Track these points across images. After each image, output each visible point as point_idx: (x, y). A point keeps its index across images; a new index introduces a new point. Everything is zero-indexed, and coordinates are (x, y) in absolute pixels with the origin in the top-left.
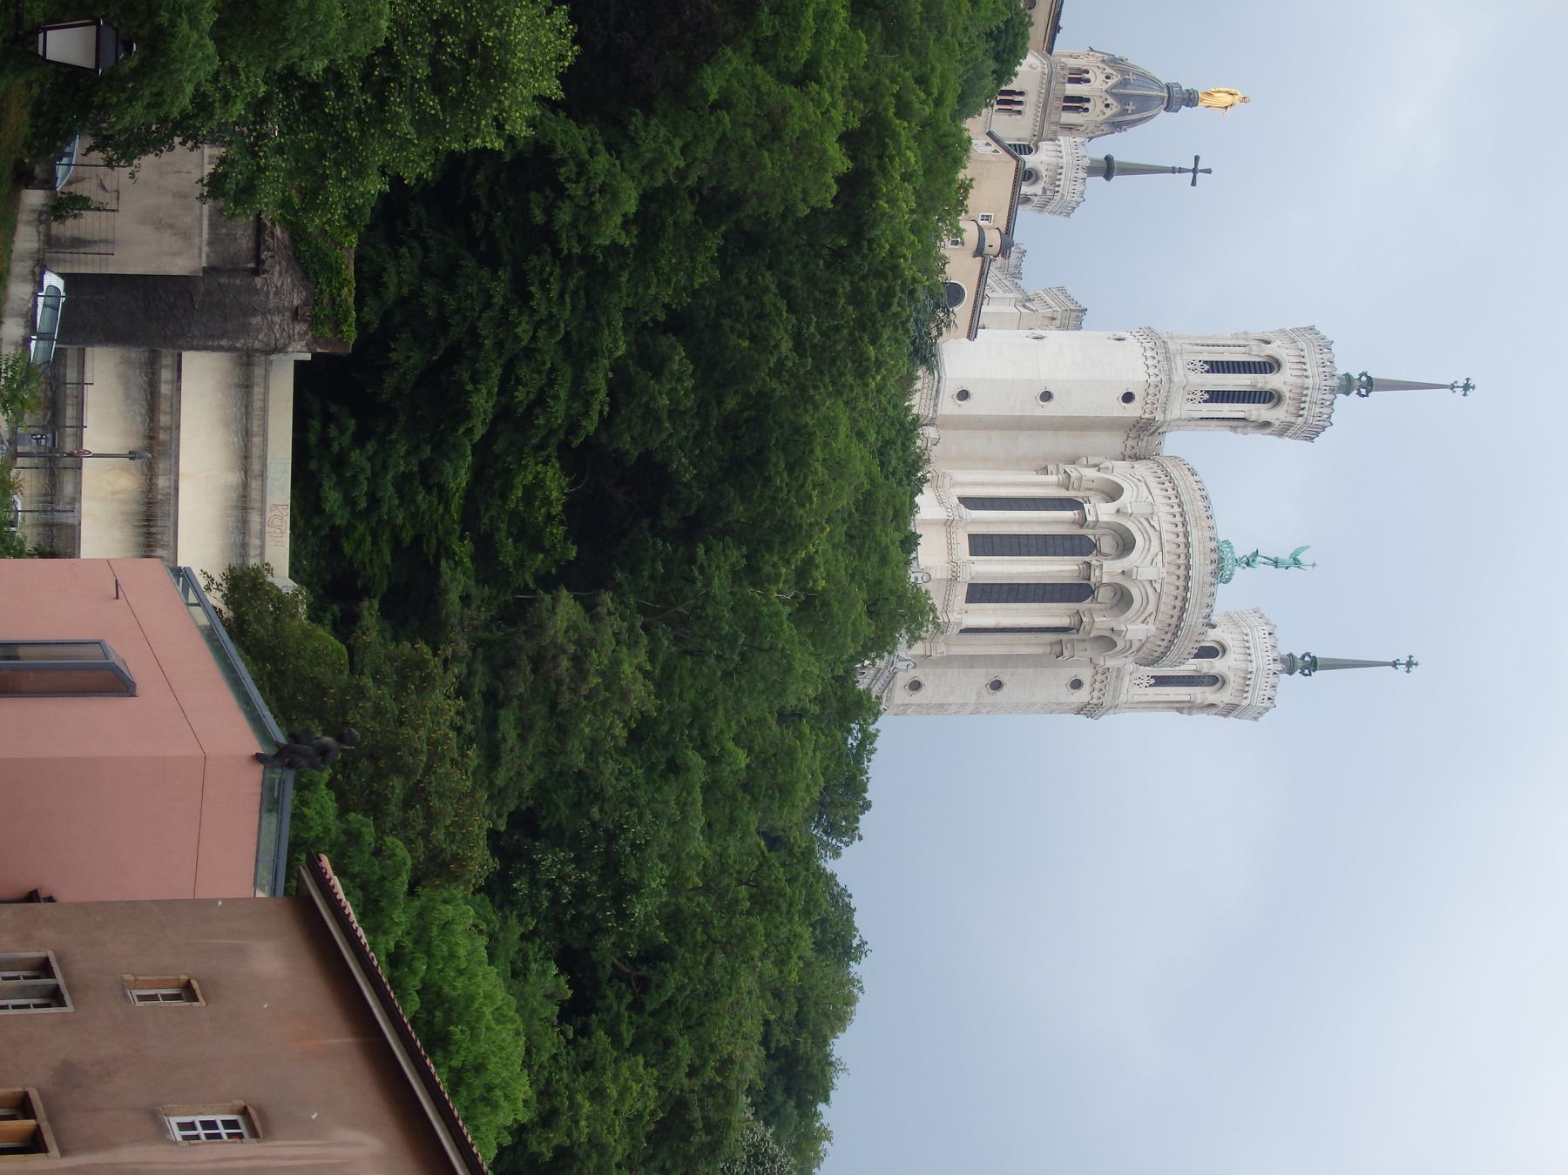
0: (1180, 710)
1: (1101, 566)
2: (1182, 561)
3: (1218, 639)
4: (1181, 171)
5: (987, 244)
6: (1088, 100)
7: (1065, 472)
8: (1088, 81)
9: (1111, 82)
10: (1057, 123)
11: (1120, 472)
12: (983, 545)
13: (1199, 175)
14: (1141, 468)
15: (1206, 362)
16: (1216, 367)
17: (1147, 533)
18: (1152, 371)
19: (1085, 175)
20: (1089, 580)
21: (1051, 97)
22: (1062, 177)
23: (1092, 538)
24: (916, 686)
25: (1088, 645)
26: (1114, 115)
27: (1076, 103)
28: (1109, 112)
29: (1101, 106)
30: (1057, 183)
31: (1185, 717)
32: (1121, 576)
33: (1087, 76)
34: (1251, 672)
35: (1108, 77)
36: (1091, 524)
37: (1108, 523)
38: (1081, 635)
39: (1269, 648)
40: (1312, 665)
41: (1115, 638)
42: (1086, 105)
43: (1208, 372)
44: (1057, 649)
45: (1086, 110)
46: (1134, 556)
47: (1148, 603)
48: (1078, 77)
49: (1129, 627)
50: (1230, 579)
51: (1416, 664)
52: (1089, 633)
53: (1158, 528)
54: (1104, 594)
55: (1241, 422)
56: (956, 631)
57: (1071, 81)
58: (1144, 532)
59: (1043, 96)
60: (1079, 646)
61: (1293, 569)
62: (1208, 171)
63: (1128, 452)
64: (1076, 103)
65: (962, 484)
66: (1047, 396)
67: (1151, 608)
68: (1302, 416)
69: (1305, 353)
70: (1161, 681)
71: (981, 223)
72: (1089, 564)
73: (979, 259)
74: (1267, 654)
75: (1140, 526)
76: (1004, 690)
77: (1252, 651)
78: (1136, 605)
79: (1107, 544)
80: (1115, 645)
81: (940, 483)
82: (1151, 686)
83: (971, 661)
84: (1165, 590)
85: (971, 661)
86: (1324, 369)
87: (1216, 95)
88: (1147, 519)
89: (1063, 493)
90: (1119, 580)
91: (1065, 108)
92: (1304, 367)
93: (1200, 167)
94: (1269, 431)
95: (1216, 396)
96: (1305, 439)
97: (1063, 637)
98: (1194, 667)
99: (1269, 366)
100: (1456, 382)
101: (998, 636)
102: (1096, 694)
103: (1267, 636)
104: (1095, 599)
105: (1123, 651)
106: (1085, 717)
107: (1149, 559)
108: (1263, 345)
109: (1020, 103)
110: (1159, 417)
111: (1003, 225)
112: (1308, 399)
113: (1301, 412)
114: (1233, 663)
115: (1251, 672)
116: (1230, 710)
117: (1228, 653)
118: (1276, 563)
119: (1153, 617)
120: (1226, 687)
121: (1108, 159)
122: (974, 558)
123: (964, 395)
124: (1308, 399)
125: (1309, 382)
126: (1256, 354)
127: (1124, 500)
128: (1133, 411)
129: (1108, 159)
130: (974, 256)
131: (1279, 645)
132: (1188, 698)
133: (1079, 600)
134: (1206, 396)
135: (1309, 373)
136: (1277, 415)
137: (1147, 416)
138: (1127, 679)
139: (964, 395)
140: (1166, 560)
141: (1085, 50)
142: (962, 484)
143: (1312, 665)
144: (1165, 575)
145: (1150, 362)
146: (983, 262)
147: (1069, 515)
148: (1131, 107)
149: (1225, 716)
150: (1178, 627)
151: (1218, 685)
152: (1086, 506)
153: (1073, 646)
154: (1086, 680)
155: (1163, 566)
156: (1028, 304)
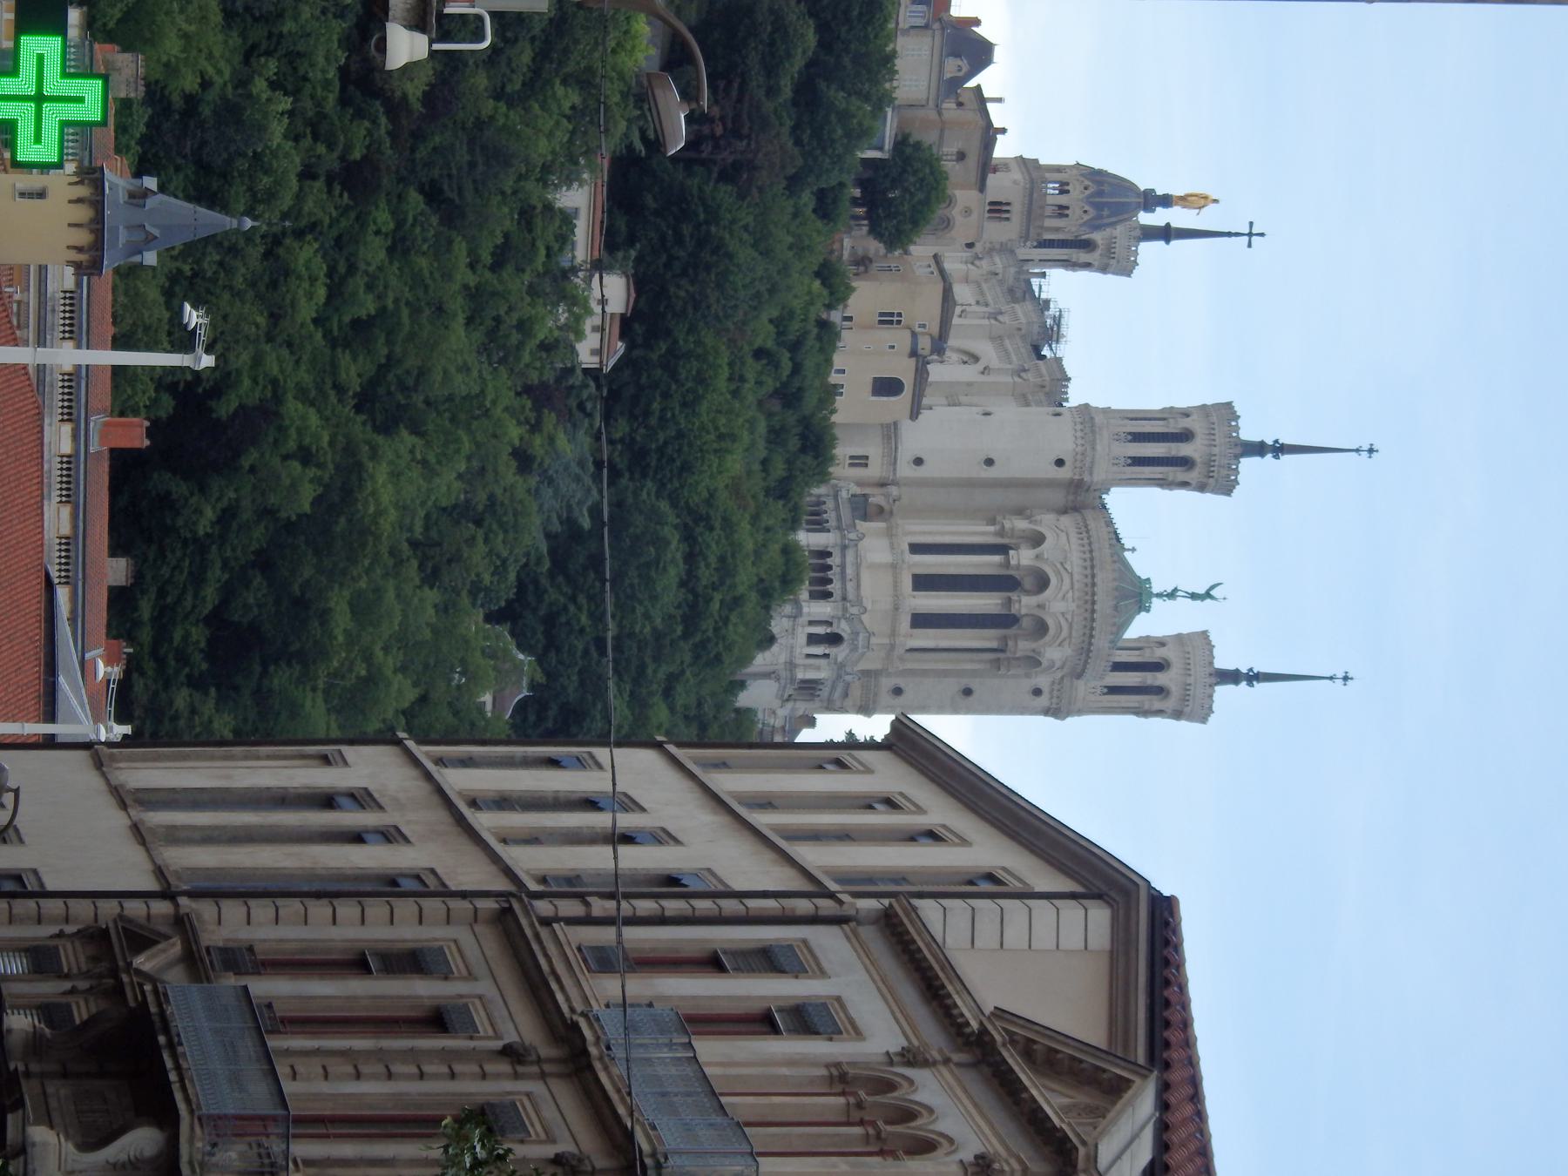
1: (1020, 601)
2: (1088, 598)
4: (1237, 234)
5: (920, 347)
6: (1067, 208)
9: (1087, 192)
11: (1046, 523)
12: (924, 582)
14: (1067, 521)
15: (1130, 433)
16: (1138, 437)
18: (1080, 441)
22: (1117, 245)
24: (898, 691)
26: (1091, 219)
28: (1086, 217)
29: (1079, 212)
31: (1142, 720)
35: (1086, 188)
38: (1008, 654)
42: (1066, 212)
43: (1130, 441)
45: (1067, 216)
46: (1048, 593)
51: (1352, 679)
54: (1026, 623)
55: (1163, 483)
56: (902, 651)
58: (1058, 573)
62: (1262, 235)
65: (914, 533)
67: (1065, 633)
69: (1215, 426)
71: (918, 330)
72: (1010, 599)
73: (914, 359)
78: (1052, 631)
79: (1028, 583)
80: (1039, 663)
81: (894, 532)
84: (1075, 620)
87: (1189, 198)
88: (1062, 564)
89: (999, 541)
92: (1213, 437)
98: (1139, 680)
99: (1185, 436)
101: (945, 655)
102: (1054, 700)
107: (1060, 595)
109: (1008, 211)
110: (1087, 478)
111: (935, 330)
112: (1216, 463)
113: (1211, 474)
116: (1178, 715)
118: (1194, 596)
119: (1067, 641)
122: (915, 593)
125: (1216, 450)
128: (1064, 473)
134: (1129, 461)
136: (1193, 476)
137: (1077, 477)
139: (919, 461)
145: (1079, 434)
146: (917, 362)
147: (997, 558)
148: (1106, 212)
150: (1089, 651)
154: (1046, 690)
155: (1073, 601)
156: (1023, 374)
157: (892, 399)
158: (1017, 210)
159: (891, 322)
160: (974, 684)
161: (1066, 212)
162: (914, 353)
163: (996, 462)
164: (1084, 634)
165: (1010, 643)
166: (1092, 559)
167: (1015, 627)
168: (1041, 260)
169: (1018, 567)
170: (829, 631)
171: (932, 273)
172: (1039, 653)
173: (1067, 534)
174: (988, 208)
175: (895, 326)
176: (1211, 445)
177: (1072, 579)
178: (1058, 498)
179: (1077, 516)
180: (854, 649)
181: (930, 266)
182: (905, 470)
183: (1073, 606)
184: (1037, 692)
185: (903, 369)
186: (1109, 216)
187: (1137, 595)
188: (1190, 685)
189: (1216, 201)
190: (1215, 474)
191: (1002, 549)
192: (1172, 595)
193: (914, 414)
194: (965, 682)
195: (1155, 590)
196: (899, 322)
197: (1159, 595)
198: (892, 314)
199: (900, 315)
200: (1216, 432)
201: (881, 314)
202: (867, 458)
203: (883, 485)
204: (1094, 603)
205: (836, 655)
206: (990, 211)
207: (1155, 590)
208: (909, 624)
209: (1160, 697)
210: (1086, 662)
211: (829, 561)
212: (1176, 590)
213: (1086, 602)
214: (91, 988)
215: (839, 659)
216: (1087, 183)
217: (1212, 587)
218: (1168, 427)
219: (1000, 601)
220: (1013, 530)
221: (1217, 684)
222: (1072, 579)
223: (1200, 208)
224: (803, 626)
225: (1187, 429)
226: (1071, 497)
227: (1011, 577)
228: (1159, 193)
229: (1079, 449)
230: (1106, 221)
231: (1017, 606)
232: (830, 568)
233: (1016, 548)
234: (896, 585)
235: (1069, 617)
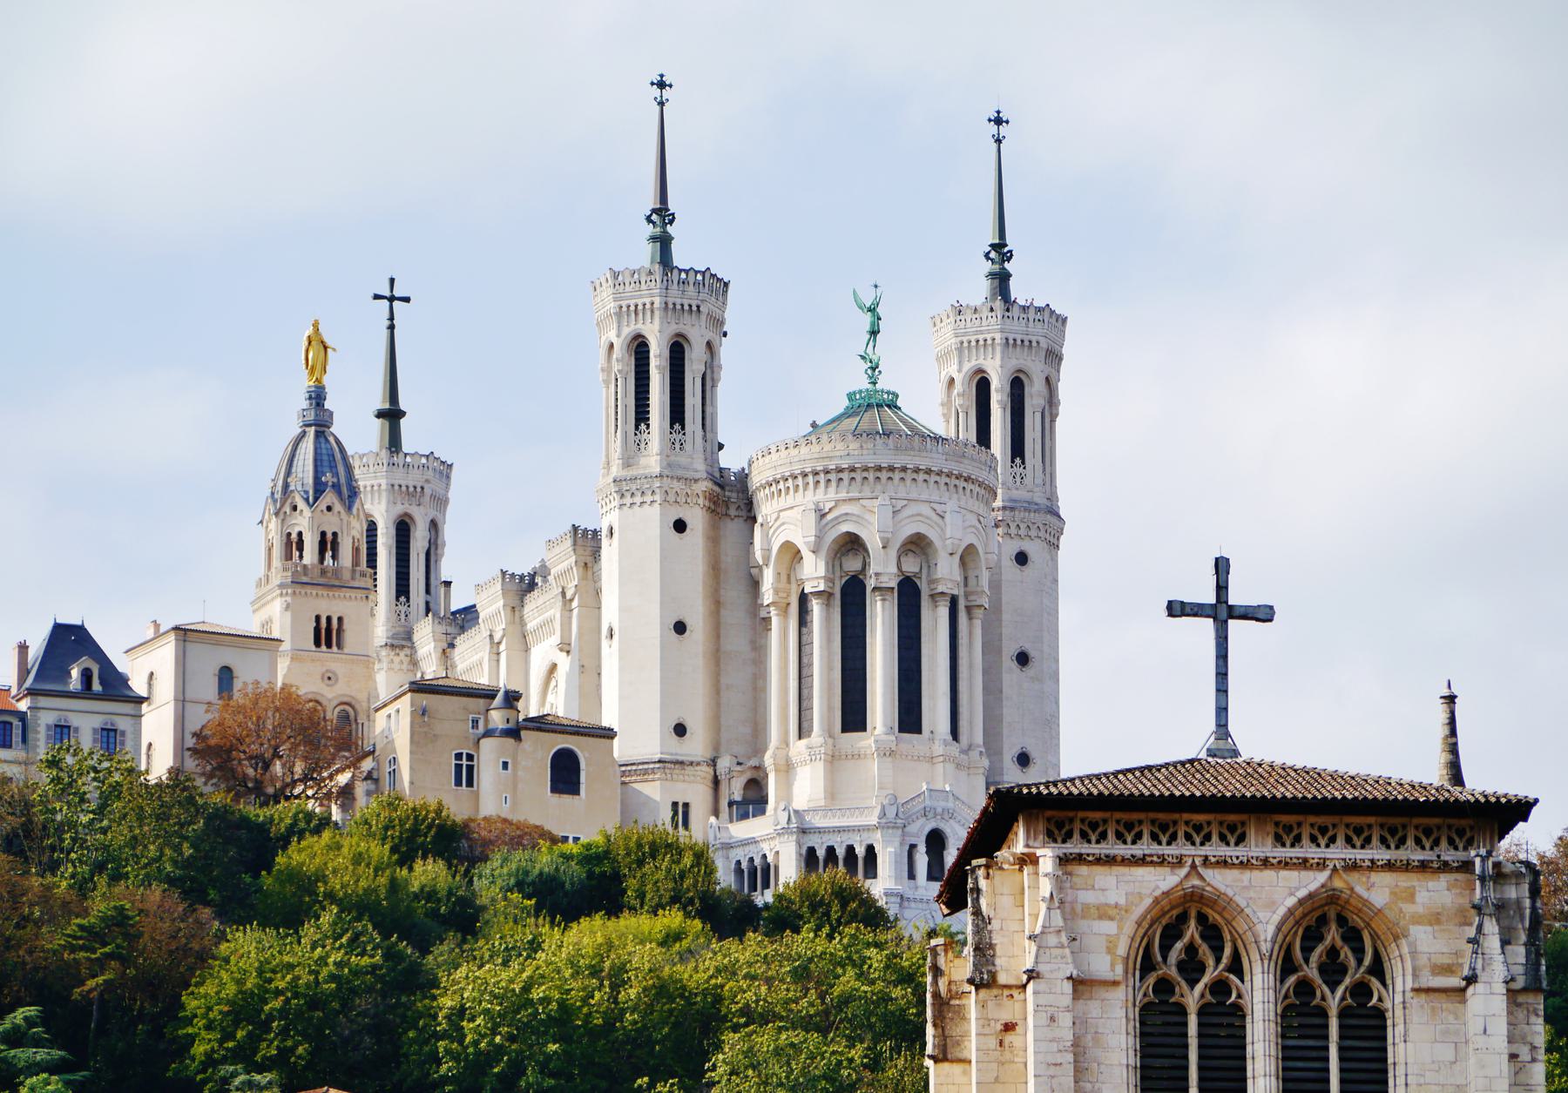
0: (1053, 421)
1: (877, 574)
2: (871, 476)
4: (392, 318)
5: (505, 726)
8: (300, 534)
10: (354, 571)
12: (854, 716)
13: (397, 293)
15: (637, 428)
16: (642, 415)
17: (836, 518)
18: (648, 498)
19: (401, 455)
20: (893, 588)
21: (322, 581)
23: (843, 582)
25: (971, 574)
28: (338, 507)
30: (411, 489)
32: (888, 550)
33: (294, 536)
34: (1007, 339)
35: (295, 508)
36: (831, 585)
37: (827, 563)
39: (977, 316)
42: (329, 536)
43: (648, 426)
45: (335, 534)
48: (294, 545)
49: (948, 536)
50: (893, 394)
53: (833, 504)
54: (911, 566)
59: (320, 593)
62: (392, 281)
63: (744, 513)
66: (680, 628)
67: (925, 510)
68: (698, 307)
71: (481, 729)
72: (875, 589)
73: (523, 733)
74: (984, 319)
75: (830, 526)
77: (981, 337)
78: (923, 529)
79: (853, 565)
80: (970, 547)
82: (1023, 463)
83: (993, 690)
84: (903, 495)
85: (993, 690)
86: (643, 283)
90: (893, 553)
93: (388, 294)
94: (715, 343)
96: (725, 292)
99: (640, 349)
100: (656, 99)
103: (962, 317)
104: (918, 575)
106: (1062, 538)
109: (329, 619)
112: (678, 301)
113: (694, 308)
114: (998, 361)
115: (1007, 339)
116: (1054, 357)
118: (874, 333)
119: (935, 506)
120: (1025, 369)
123: (680, 730)
124: (678, 301)
126: (623, 364)
128: (697, 518)
129: (380, 414)
131: (973, 304)
133: (917, 592)
134: (677, 426)
135: (647, 301)
136: (697, 335)
137: (701, 501)
139: (680, 730)
140: (870, 495)
141: (261, 529)
142: (786, 733)
144: (886, 496)
145: (638, 499)
146: (527, 728)
147: (816, 607)
148: (328, 478)
149: (1061, 359)
151: (1022, 376)
153: (972, 593)
156: (569, 596)
159: (470, 769)
160: (1010, 650)
161: (329, 536)
162: (514, 733)
163: (681, 618)
165: (940, 589)
168: (428, 591)
169: (829, 580)
170: (922, 848)
171: (398, 711)
173: (781, 511)
174: (324, 648)
175: (475, 763)
178: (733, 528)
179: (760, 497)
181: (389, 716)
184: (1022, 559)
185: (538, 752)
186: (336, 475)
189: (316, 325)
191: (803, 599)
194: (1009, 664)
195: (863, 384)
198: (459, 767)
200: (632, 302)
201: (458, 783)
202: (675, 804)
203: (716, 782)
204: (879, 469)
206: (329, 645)
207: (863, 384)
211: (821, 853)
214: (181, 879)
216: (287, 509)
223: (325, 348)
224: (917, 888)
230: (343, 480)
231: (884, 579)
232: (831, 851)
233: (801, 582)
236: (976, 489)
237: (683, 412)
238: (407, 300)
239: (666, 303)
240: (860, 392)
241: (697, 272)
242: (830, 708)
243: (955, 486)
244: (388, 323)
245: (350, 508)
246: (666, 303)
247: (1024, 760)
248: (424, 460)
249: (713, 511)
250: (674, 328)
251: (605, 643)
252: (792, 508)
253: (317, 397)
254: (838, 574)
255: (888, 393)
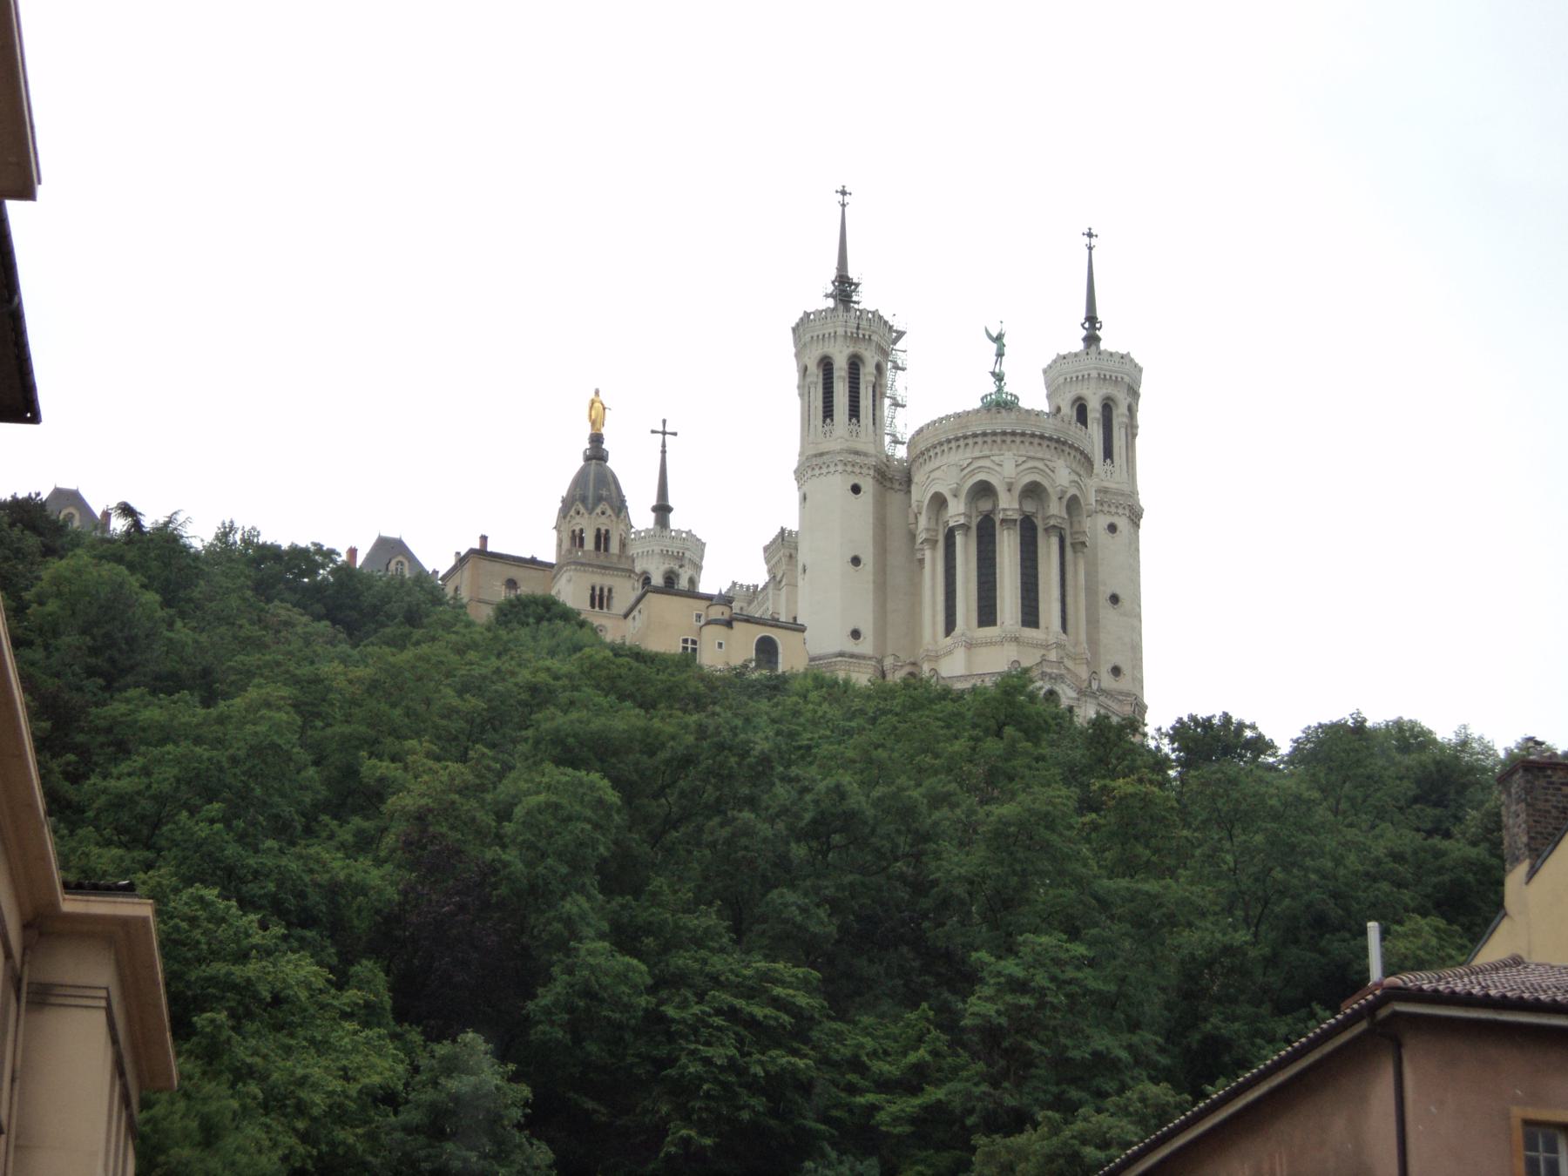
0: (1134, 435)
1: (1005, 510)
2: (999, 439)
3: (1070, 402)
4: (664, 446)
5: (720, 617)
7: (922, 543)
9: (582, 510)
11: (921, 494)
12: (987, 615)
13: (667, 430)
14: (918, 477)
15: (824, 422)
16: (828, 412)
18: (832, 469)
19: (668, 531)
20: (1016, 520)
21: (595, 562)
23: (979, 519)
24: (1116, 671)
25: (1075, 519)
27: (602, 539)
28: (609, 512)
29: (603, 519)
31: (1140, 431)
33: (577, 532)
35: (578, 513)
38: (1066, 526)
40: (1091, 319)
41: (1068, 495)
42: (603, 531)
43: (832, 420)
44: (1079, 547)
45: (607, 531)
46: (995, 481)
47: (1035, 468)
48: (577, 539)
52: (1064, 519)
54: (1030, 507)
57: (581, 545)
58: (972, 473)
60: (1076, 528)
61: (1005, 341)
62: (664, 422)
63: (904, 487)
64: (602, 539)
66: (856, 561)
67: (1040, 465)
68: (870, 336)
70: (1108, 453)
71: (703, 622)
72: (1003, 521)
73: (735, 624)
76: (1118, 592)
79: (985, 506)
82: (1113, 462)
84: (1024, 453)
85: (1093, 622)
88: (962, 470)
91: (606, 549)
92: (827, 336)
95: (854, 411)
97: (1068, 542)
98: (1095, 425)
99: (826, 365)
101: (1069, 600)
102: (1120, 511)
105: (1080, 488)
107: (997, 468)
108: (808, 373)
109: (602, 590)
116: (1134, 393)
117: (1083, 396)
118: (1000, 355)
119: (1048, 463)
121: (655, 509)
122: (999, 623)
123: (856, 634)
125: (841, 331)
126: (816, 375)
127: (945, 491)
128: (868, 485)
129: (655, 509)
130: (732, 628)
132: (1123, 431)
133: (1034, 528)
134: (854, 420)
135: (832, 331)
136: (870, 358)
137: (872, 472)
138: (1106, 484)
139: (856, 634)
140: (997, 452)
143: (1091, 319)
145: (824, 470)
147: (959, 539)
149: (1139, 396)
150: (1058, 441)
151: (1111, 404)
152: (951, 524)
153: (1077, 533)
154: (1109, 519)
156: (778, 579)
157: (780, 650)
158: (601, 580)
160: (1105, 592)
161: (603, 531)
162: (729, 624)
164: (1040, 444)
165: (1052, 522)
166: (957, 439)
167: (1035, 520)
172: (1064, 492)
174: (597, 609)
175: (697, 646)
176: (835, 337)
177: (979, 458)
180: (1059, 678)
182: (866, 646)
183: (1009, 455)
186: (609, 490)
187: (1001, 404)
188: (1099, 375)
189: (597, 393)
190: (867, 333)
192: (999, 377)
193: (796, 627)
196: (694, 642)
197: (1000, 389)
199: (685, 641)
205: (1068, 698)
206: (601, 607)
208: (1034, 630)
209: (1114, 408)
210: (1071, 446)
212: (993, 374)
213: (1004, 441)
215: (1074, 695)
217: (990, 336)
218: (816, 383)
219: (1005, 532)
220: (928, 530)
221: (1098, 347)
222: (979, 458)
225: (819, 365)
226: (897, 486)
227: (980, 527)
228: (588, 446)
229: (840, 468)
231: (1009, 513)
234: (989, 643)
235: (1021, 460)
236: (1078, 456)
237: (858, 412)
238: (675, 434)
239: (846, 332)
240: (991, 395)
241: (868, 312)
242: (968, 610)
243: (1063, 451)
244: (661, 449)
245: (618, 516)
246: (846, 332)
247: (1116, 671)
248: (684, 535)
249: (881, 483)
250: (851, 350)
251: (800, 577)
252: (939, 467)
253: (597, 439)
254: (974, 514)
255: (1011, 395)
